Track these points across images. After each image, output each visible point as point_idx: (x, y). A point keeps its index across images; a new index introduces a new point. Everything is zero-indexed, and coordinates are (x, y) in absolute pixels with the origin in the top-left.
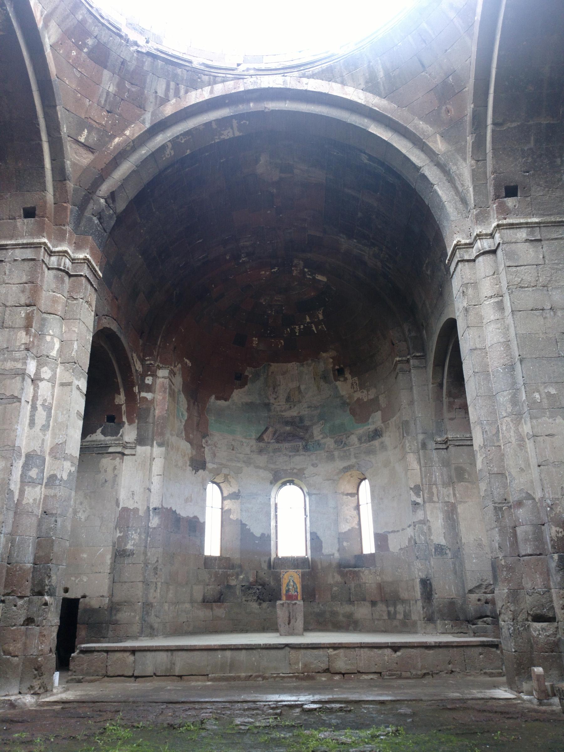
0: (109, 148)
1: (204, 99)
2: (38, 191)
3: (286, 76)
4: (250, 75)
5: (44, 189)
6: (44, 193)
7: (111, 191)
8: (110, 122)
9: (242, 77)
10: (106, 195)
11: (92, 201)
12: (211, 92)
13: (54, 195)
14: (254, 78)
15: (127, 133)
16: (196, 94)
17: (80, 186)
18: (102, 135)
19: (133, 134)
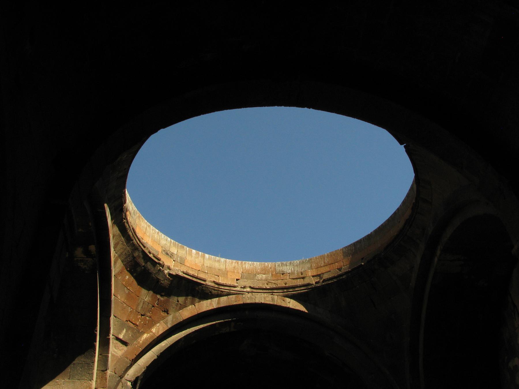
0: (139, 342)
1: (213, 308)
2: (86, 380)
3: (274, 295)
4: (247, 292)
5: (92, 379)
6: (91, 382)
7: (136, 376)
8: (142, 323)
9: (240, 292)
10: (133, 379)
11: (121, 384)
12: (219, 303)
13: (96, 381)
14: (250, 294)
15: (154, 330)
16: (207, 303)
17: (115, 373)
18: (135, 332)
19: (158, 332)
